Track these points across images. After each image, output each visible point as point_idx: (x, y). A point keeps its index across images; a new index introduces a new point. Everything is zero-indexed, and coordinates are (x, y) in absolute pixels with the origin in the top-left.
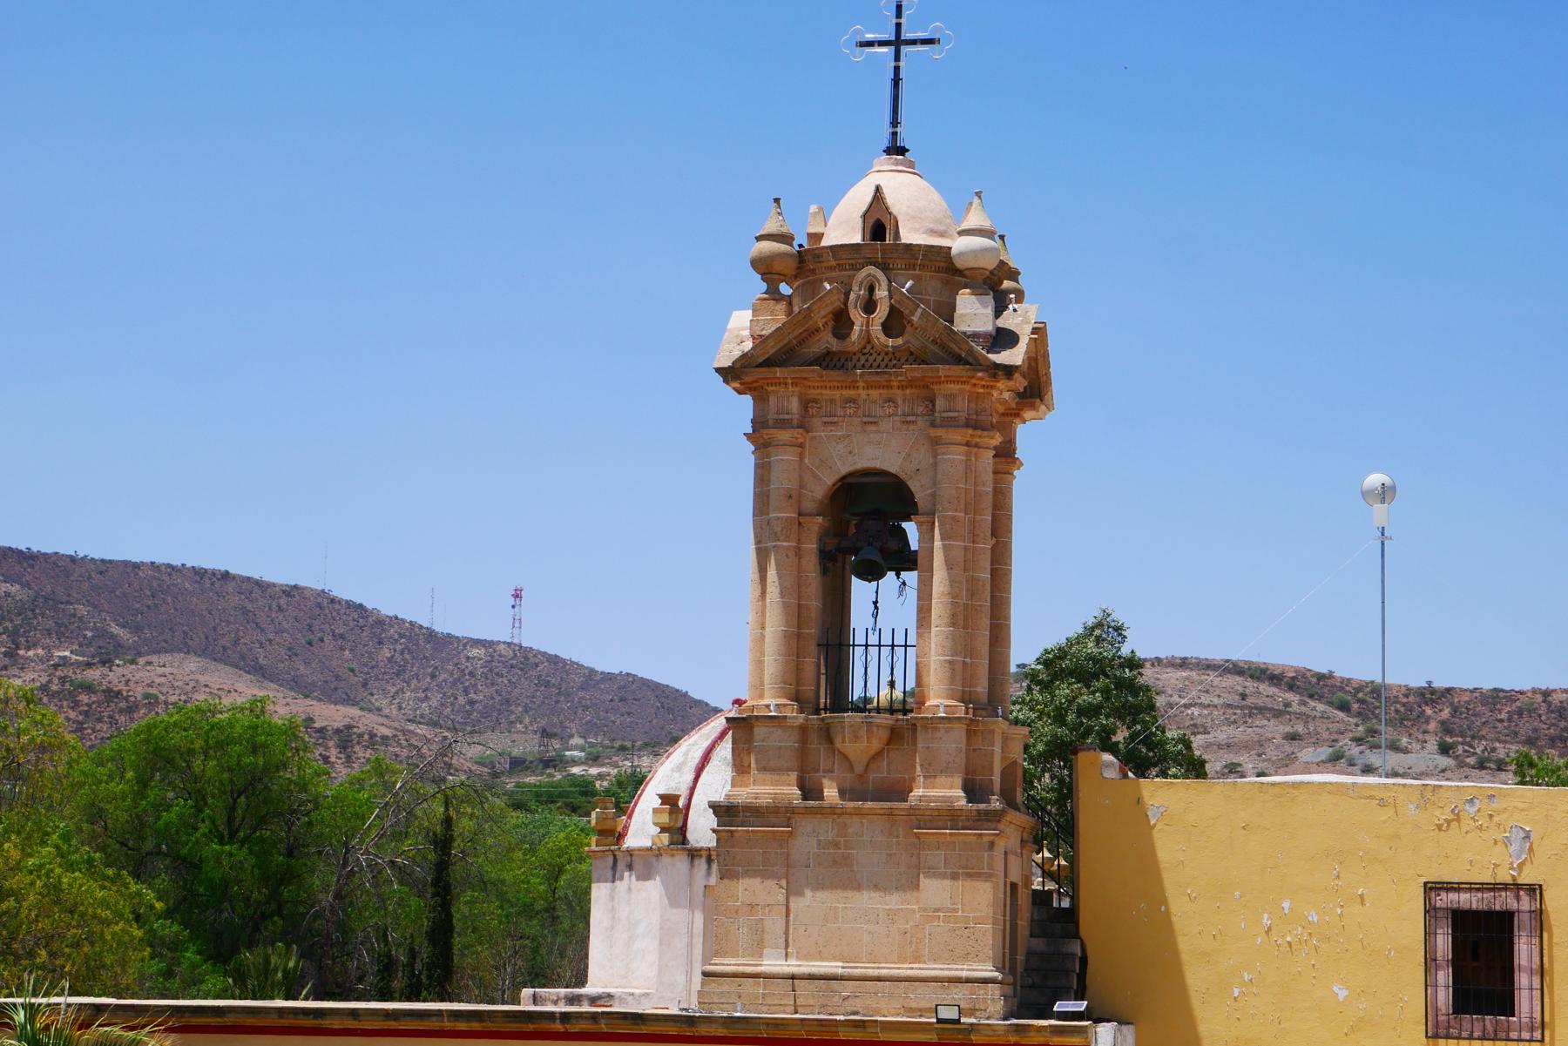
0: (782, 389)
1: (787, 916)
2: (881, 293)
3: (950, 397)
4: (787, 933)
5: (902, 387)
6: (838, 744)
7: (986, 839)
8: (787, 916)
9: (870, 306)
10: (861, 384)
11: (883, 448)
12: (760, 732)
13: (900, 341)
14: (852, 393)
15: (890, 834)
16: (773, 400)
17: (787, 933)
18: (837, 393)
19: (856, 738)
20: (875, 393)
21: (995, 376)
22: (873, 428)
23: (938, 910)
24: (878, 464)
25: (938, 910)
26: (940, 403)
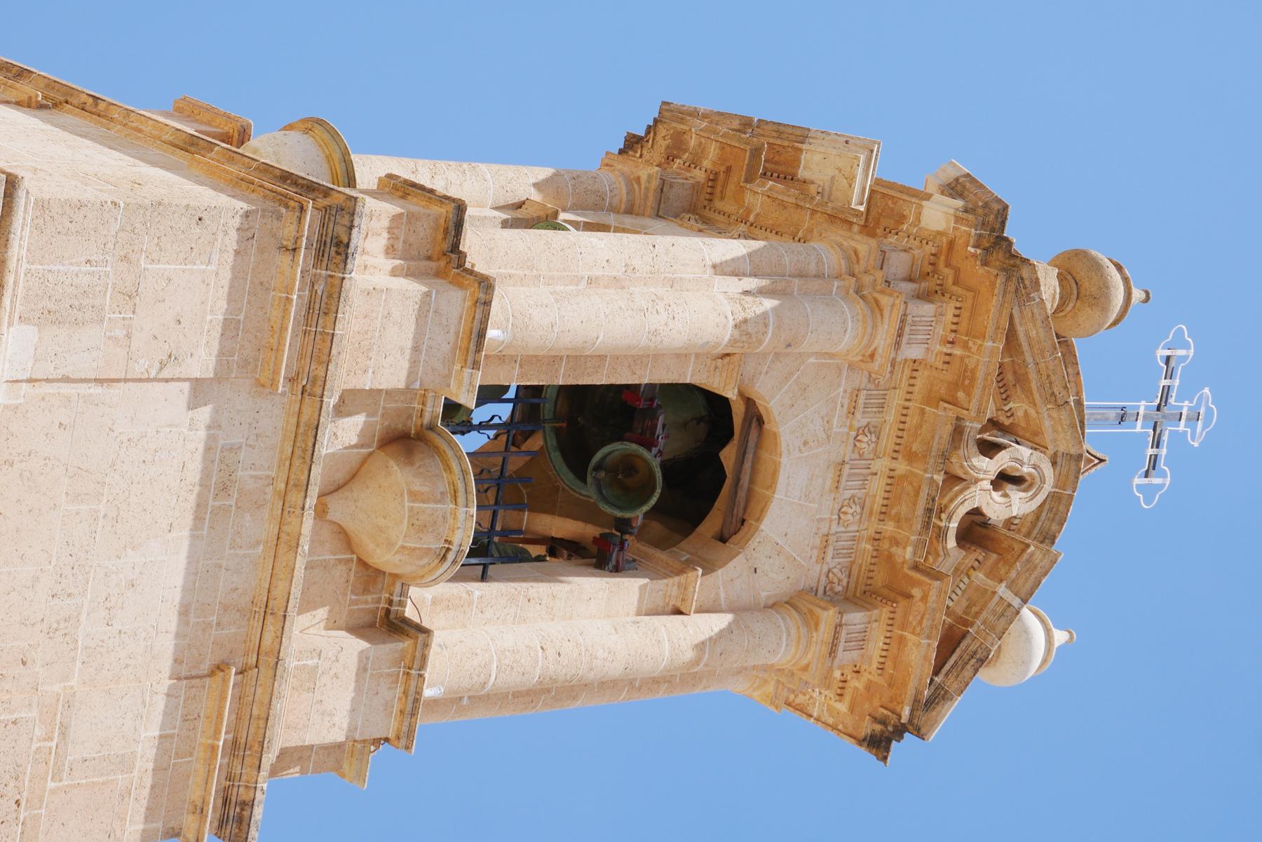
0: (940, 331)
1: (99, 381)
2: (1018, 504)
3: (861, 641)
4: (66, 380)
5: (877, 539)
6: (397, 476)
7: (189, 823)
8: (99, 381)
9: (1004, 479)
10: (902, 467)
11: (801, 503)
12: (455, 301)
13: (951, 543)
14: (888, 440)
15: (225, 608)
16: (927, 309)
17: (66, 380)
18: (891, 416)
19: (419, 528)
20: (877, 486)
21: (883, 722)
22: (829, 483)
23: (63, 734)
24: (779, 495)
25: (63, 734)
26: (856, 618)
